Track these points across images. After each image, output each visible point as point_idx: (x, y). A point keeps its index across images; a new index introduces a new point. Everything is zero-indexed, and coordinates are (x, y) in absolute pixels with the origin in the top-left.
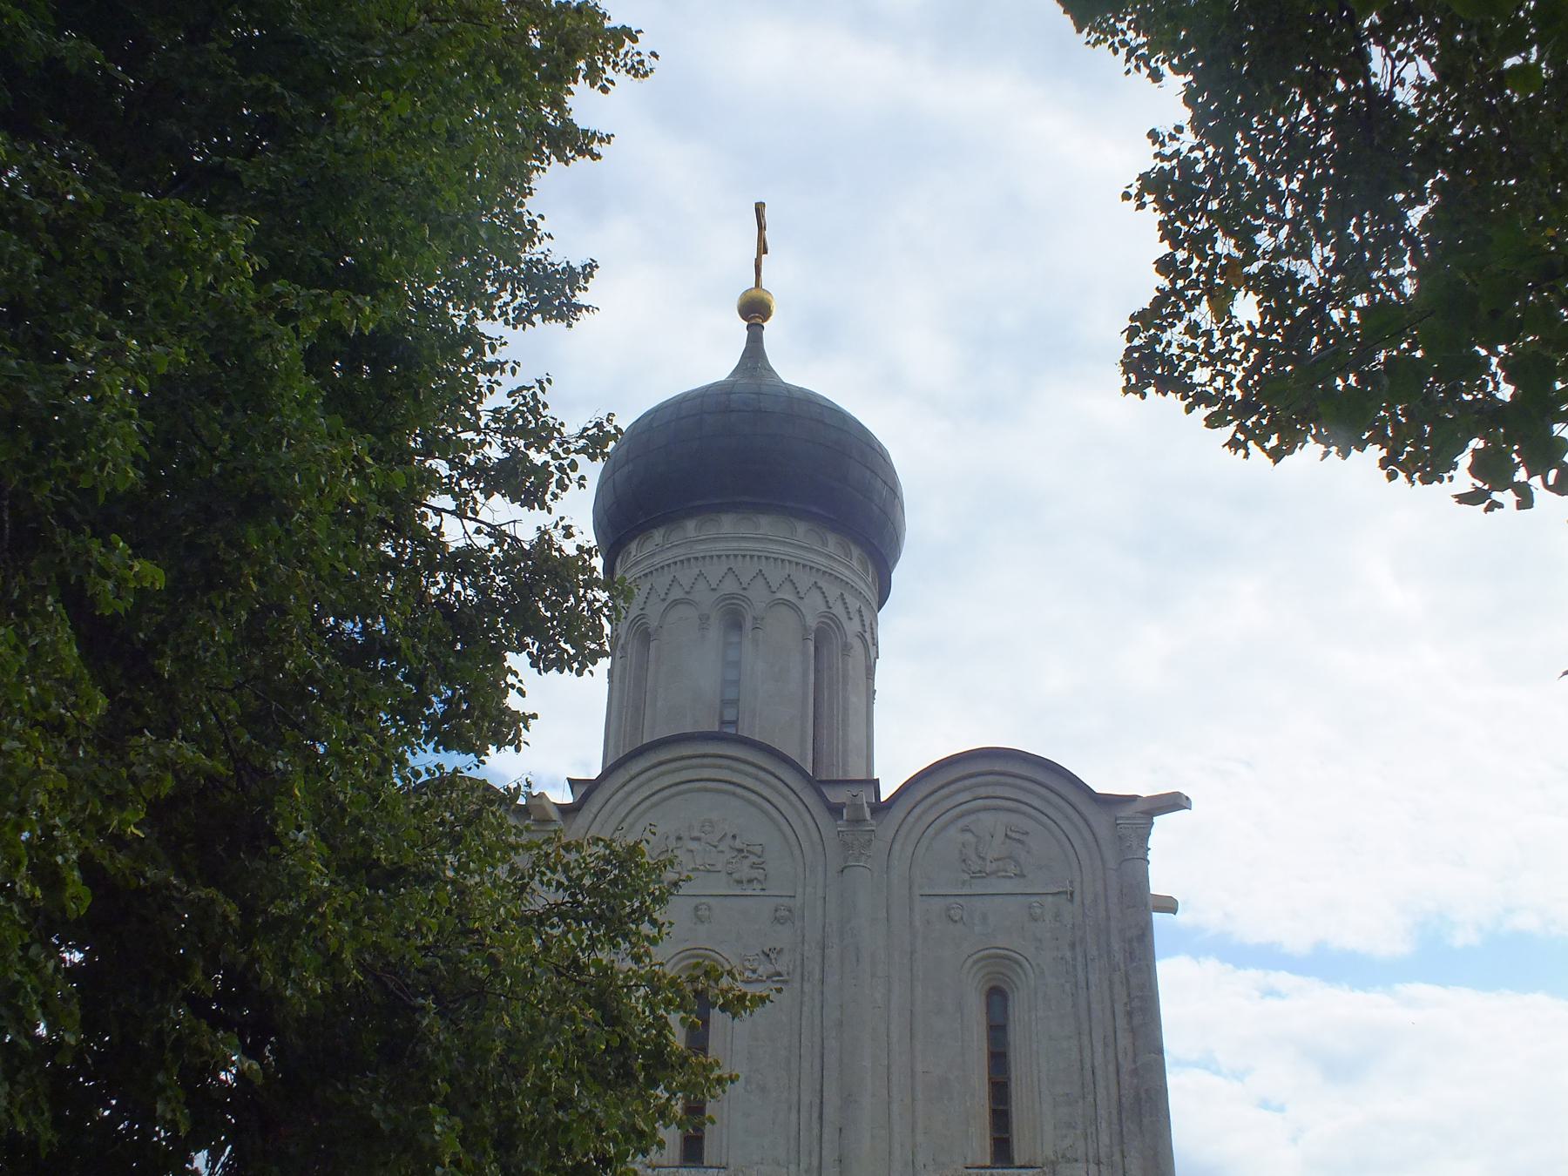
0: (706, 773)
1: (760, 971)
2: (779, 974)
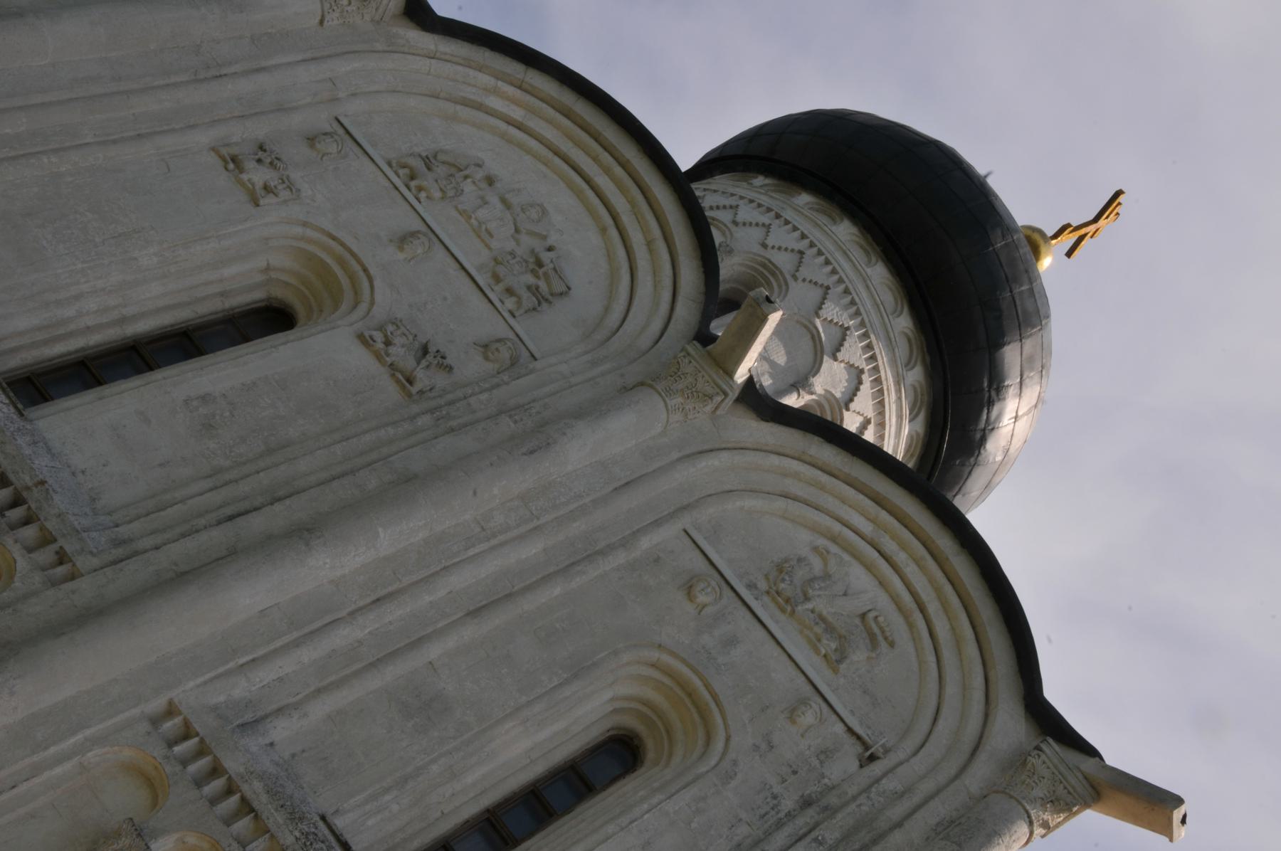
0: (602, 181)
1: (392, 350)
2: (410, 381)
